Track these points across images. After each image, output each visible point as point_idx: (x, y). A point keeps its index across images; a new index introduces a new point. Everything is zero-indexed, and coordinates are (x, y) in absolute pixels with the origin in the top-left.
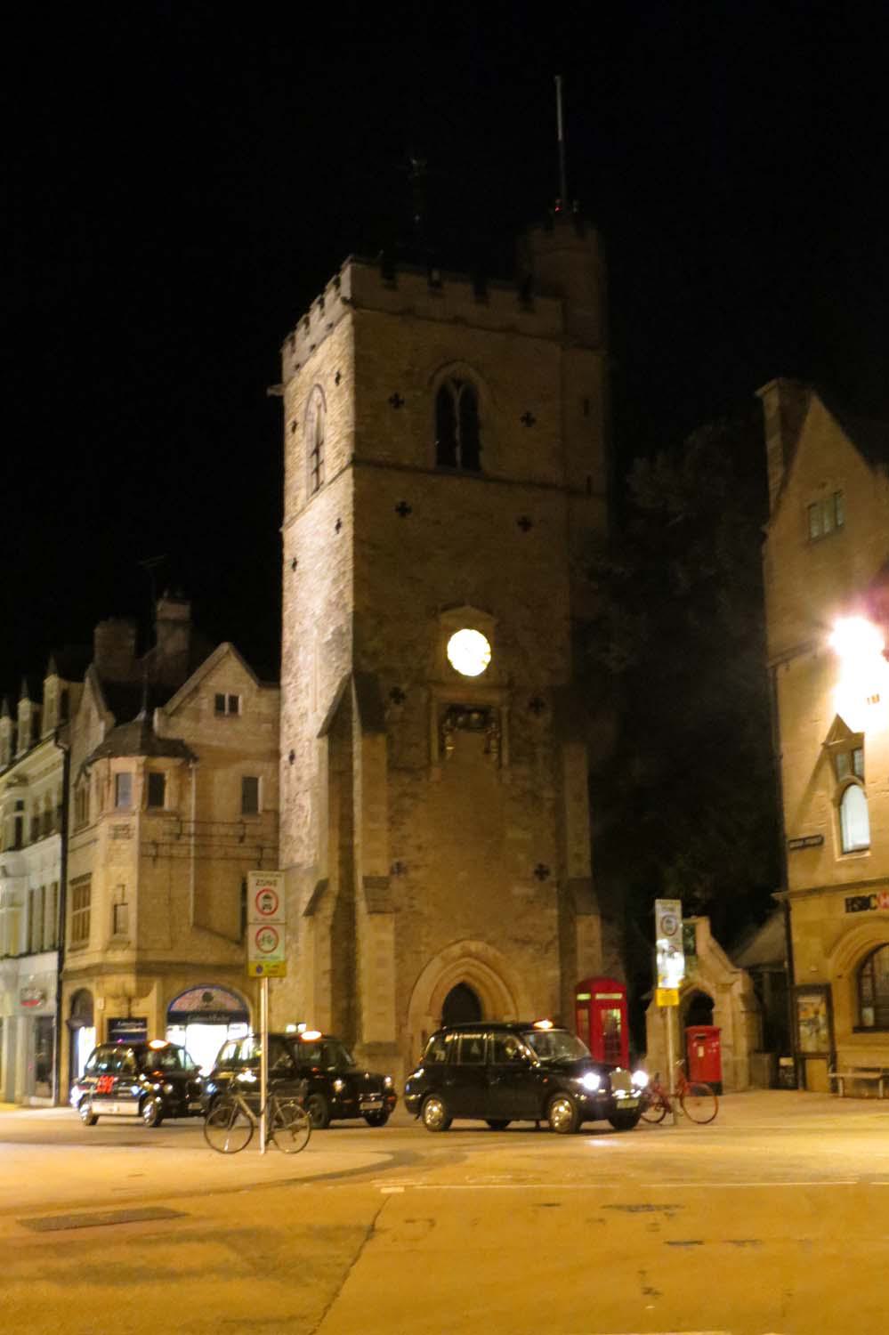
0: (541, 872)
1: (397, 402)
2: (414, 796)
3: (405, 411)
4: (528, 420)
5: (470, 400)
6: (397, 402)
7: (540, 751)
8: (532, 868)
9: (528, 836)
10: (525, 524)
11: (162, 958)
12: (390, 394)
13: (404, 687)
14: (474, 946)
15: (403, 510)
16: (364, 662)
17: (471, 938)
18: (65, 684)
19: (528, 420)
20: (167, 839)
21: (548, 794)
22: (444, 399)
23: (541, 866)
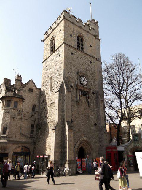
0: (95, 125)
1: (71, 36)
2: (74, 106)
4: (91, 46)
5: (82, 41)
7: (94, 101)
9: (93, 117)
10: (91, 62)
11: (13, 140)
13: (73, 85)
14: (85, 138)
16: (65, 78)
19: (91, 46)
21: (96, 110)
22: (78, 39)
23: (95, 123)
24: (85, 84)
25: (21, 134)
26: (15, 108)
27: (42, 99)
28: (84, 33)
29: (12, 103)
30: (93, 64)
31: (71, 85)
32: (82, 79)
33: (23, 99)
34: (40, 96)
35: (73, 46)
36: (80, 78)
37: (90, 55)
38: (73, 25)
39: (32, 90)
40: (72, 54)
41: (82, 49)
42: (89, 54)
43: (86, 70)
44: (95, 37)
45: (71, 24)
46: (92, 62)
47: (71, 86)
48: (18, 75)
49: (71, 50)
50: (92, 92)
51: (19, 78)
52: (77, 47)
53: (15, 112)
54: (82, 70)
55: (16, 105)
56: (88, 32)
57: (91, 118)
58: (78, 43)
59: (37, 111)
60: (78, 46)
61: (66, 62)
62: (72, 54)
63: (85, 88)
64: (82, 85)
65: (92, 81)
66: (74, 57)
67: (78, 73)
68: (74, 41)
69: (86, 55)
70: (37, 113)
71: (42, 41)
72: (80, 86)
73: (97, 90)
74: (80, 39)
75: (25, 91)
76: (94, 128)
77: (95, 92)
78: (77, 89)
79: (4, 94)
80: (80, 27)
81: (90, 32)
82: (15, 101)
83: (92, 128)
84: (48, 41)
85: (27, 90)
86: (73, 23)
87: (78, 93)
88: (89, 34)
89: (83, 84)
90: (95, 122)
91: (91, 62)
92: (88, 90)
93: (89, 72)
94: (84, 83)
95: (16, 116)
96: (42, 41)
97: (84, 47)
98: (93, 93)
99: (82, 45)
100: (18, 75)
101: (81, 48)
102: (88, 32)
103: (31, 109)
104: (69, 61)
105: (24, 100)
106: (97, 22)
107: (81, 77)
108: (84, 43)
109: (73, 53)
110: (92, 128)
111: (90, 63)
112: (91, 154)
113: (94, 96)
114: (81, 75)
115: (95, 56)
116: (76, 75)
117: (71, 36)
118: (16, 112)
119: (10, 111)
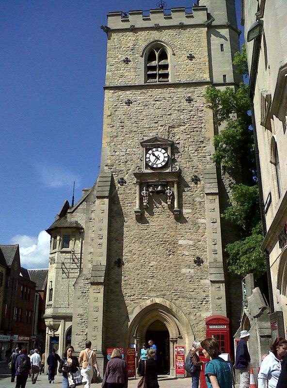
4: (191, 57)
5: (164, 56)
6: (127, 61)
8: (192, 259)
9: (191, 243)
10: (189, 100)
15: (129, 103)
17: (157, 297)
19: (191, 57)
20: (69, 261)
22: (151, 57)
23: (198, 258)
24: (160, 166)
31: (122, 179)
37: (189, 80)
41: (166, 76)
42: (183, 81)
46: (194, 97)
47: (122, 182)
57: (181, 246)
64: (152, 168)
66: (134, 107)
74: (157, 54)
76: (192, 271)
80: (158, 28)
83: (184, 271)
89: (155, 166)
90: (198, 254)
93: (182, 128)
104: (118, 124)
105: (83, 229)
110: (184, 271)
112: (181, 338)
113: (199, 186)
114: (150, 145)
118: (69, 256)
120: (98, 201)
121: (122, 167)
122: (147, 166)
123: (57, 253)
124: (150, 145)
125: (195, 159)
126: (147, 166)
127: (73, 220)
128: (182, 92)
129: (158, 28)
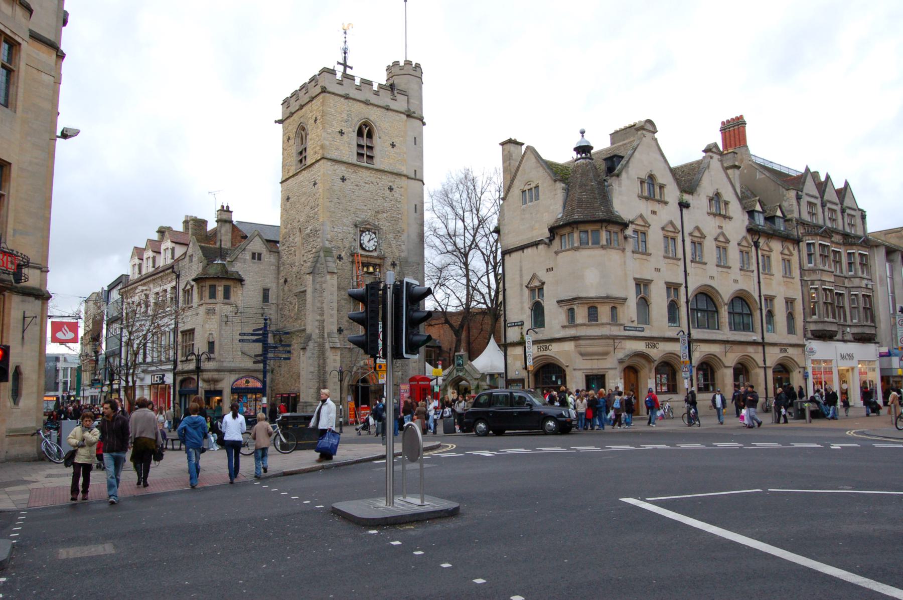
1: (341, 133)
3: (345, 136)
4: (393, 145)
5: (370, 135)
10: (391, 189)
12: (339, 129)
13: (343, 254)
18: (174, 245)
19: (393, 145)
22: (360, 133)
25: (243, 353)
26: (227, 301)
27: (282, 274)
28: (374, 115)
29: (220, 290)
30: (396, 194)
32: (366, 238)
33: (241, 281)
34: (279, 268)
35: (345, 159)
36: (361, 235)
38: (347, 101)
39: (260, 255)
40: (343, 179)
41: (371, 158)
43: (378, 212)
44: (408, 116)
45: (342, 99)
47: (340, 258)
48: (223, 207)
49: (341, 170)
50: (389, 262)
51: (225, 216)
52: (354, 159)
53: (227, 310)
54: (366, 215)
55: (227, 295)
56: (387, 109)
58: (360, 146)
59: (274, 301)
60: (360, 155)
61: (329, 204)
62: (343, 179)
63: (372, 257)
65: (391, 236)
67: (356, 226)
68: (349, 144)
69: (379, 175)
70: (274, 307)
71: (276, 122)
72: (362, 256)
73: (403, 255)
75: (245, 261)
77: (397, 262)
78: (353, 262)
79: (200, 269)
80: (367, 103)
81: (393, 105)
82: (225, 286)
84: (293, 128)
85: (248, 256)
86: (347, 97)
87: (354, 272)
88: (391, 113)
91: (391, 189)
92: (378, 261)
93: (385, 215)
94: (370, 246)
95: (230, 319)
96: (276, 122)
97: (376, 152)
98: (394, 265)
99: (370, 148)
100: (223, 207)
101: (368, 156)
102: (387, 109)
103: (261, 299)
104: (336, 200)
106: (418, 66)
107: (362, 232)
108: (377, 141)
109: (346, 176)
111: (388, 192)
114: (363, 228)
115: (404, 170)
116: (352, 230)
117: (341, 133)
119: (217, 307)
120: (328, 277)
121: (340, 244)
122: (361, 245)
123: (218, 305)
124: (363, 228)
125: (394, 246)
126: (361, 245)
127: (233, 269)
128: (386, 180)
129: (367, 103)
